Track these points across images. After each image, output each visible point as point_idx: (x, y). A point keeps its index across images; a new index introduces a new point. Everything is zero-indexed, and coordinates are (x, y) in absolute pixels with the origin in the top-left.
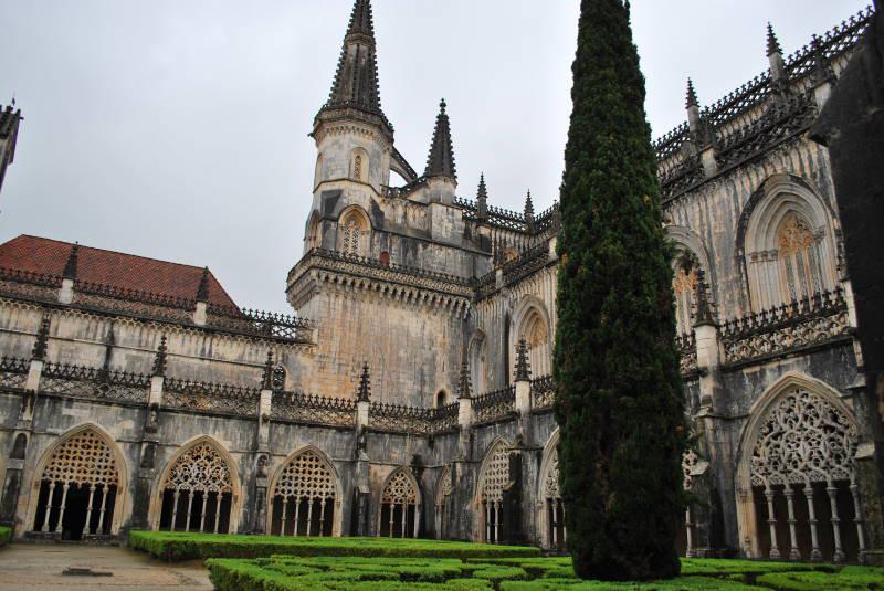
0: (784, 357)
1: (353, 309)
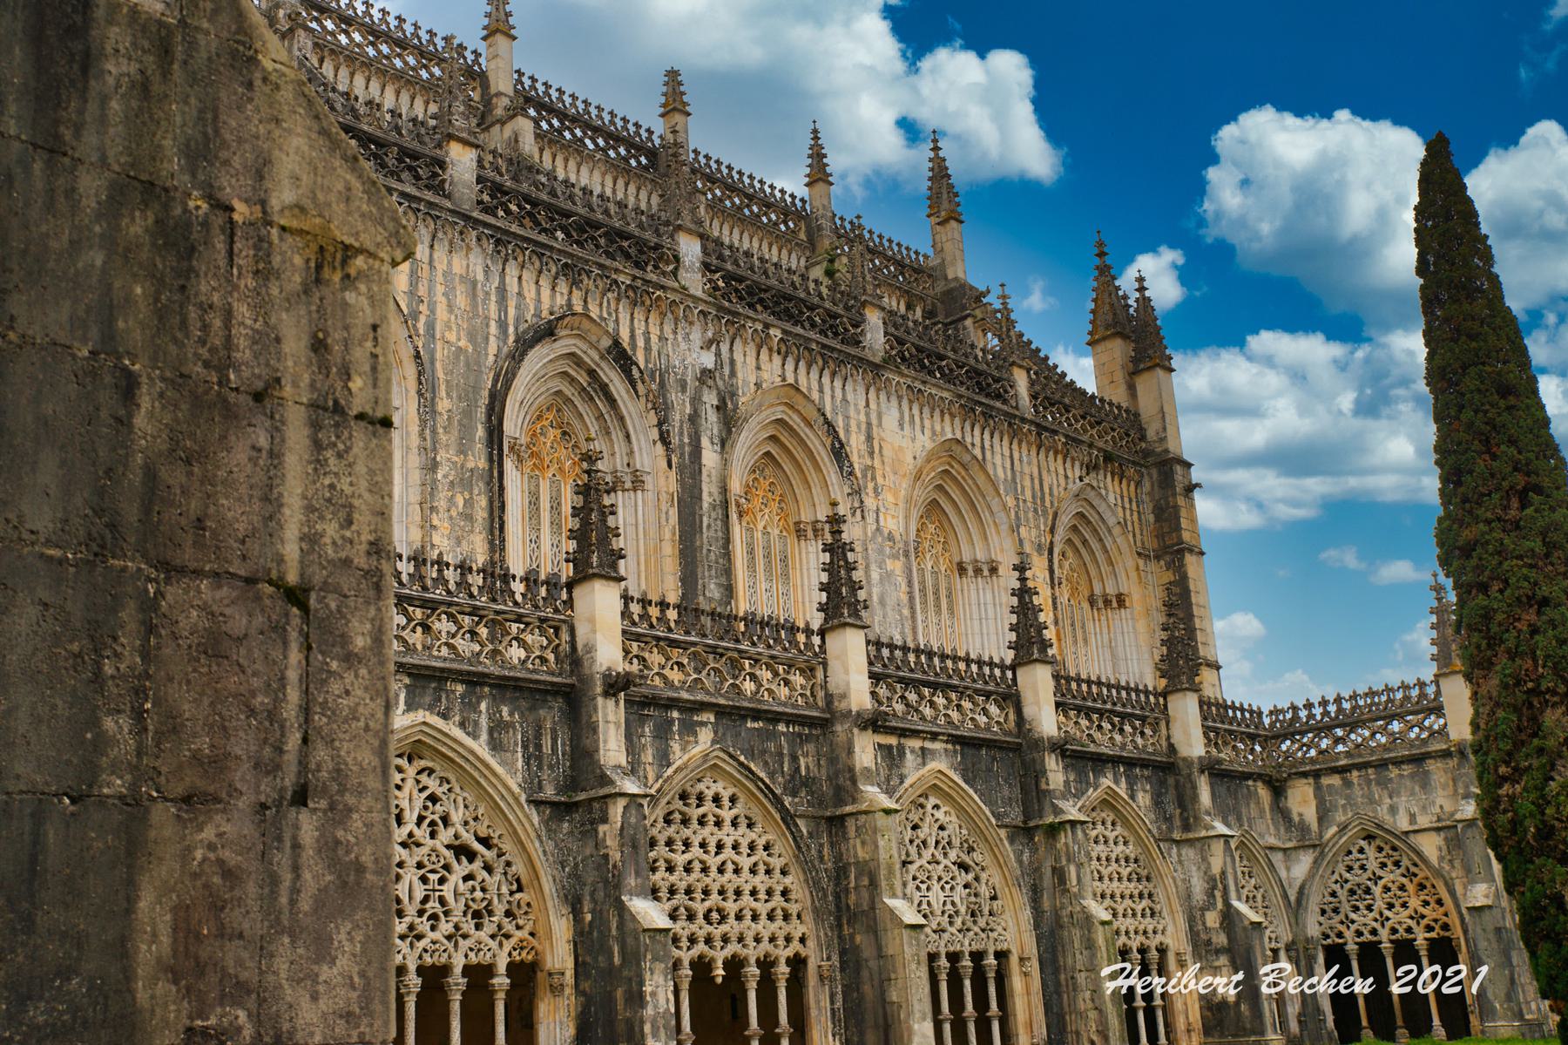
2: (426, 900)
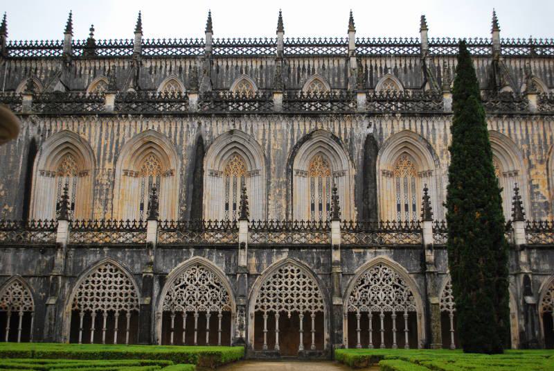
0: (380, 248)
2: (201, 297)
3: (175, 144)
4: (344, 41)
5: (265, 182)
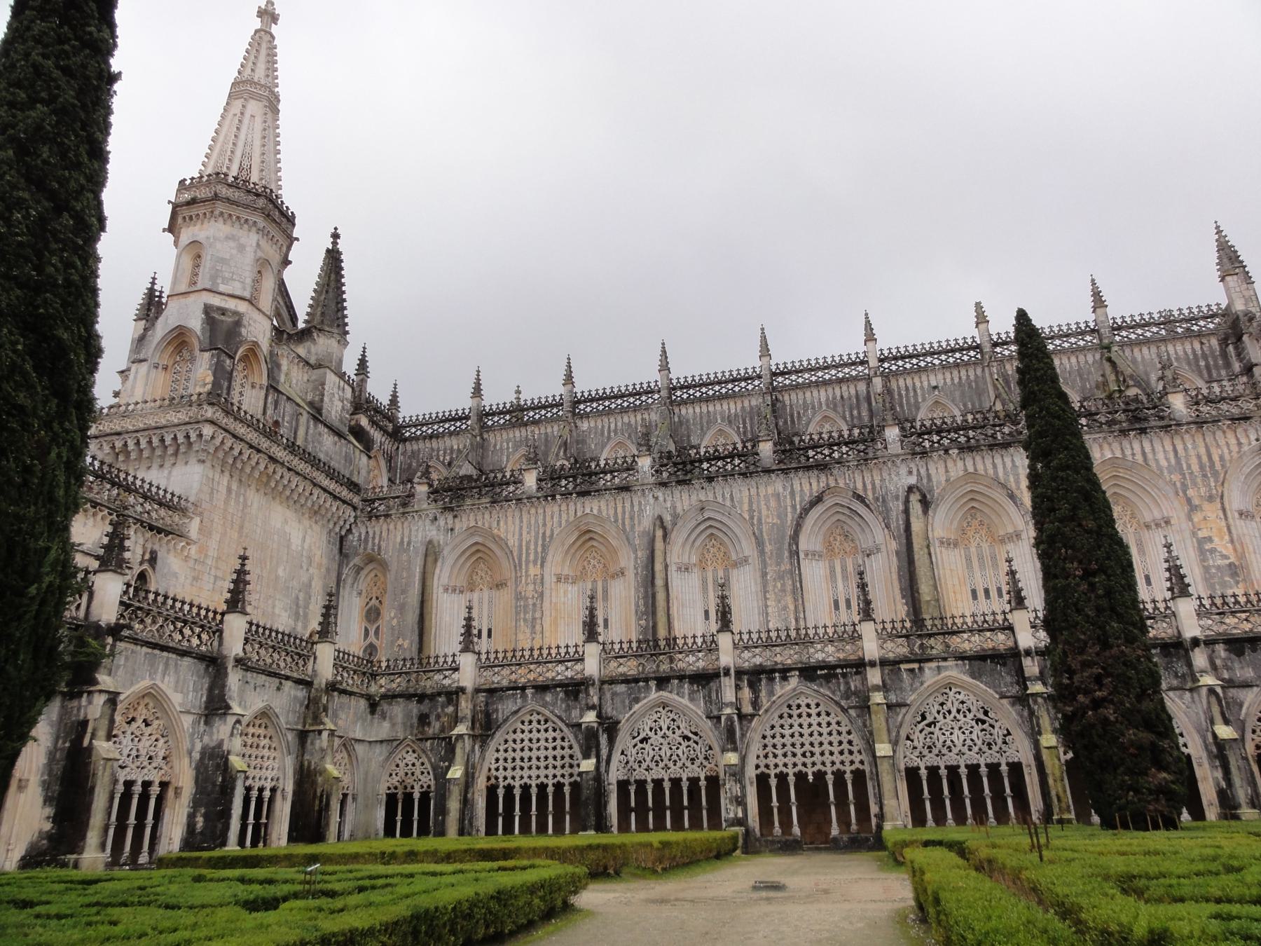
0: (945, 659)
1: (238, 495)
3: (624, 530)
4: (861, 356)
5: (758, 574)
